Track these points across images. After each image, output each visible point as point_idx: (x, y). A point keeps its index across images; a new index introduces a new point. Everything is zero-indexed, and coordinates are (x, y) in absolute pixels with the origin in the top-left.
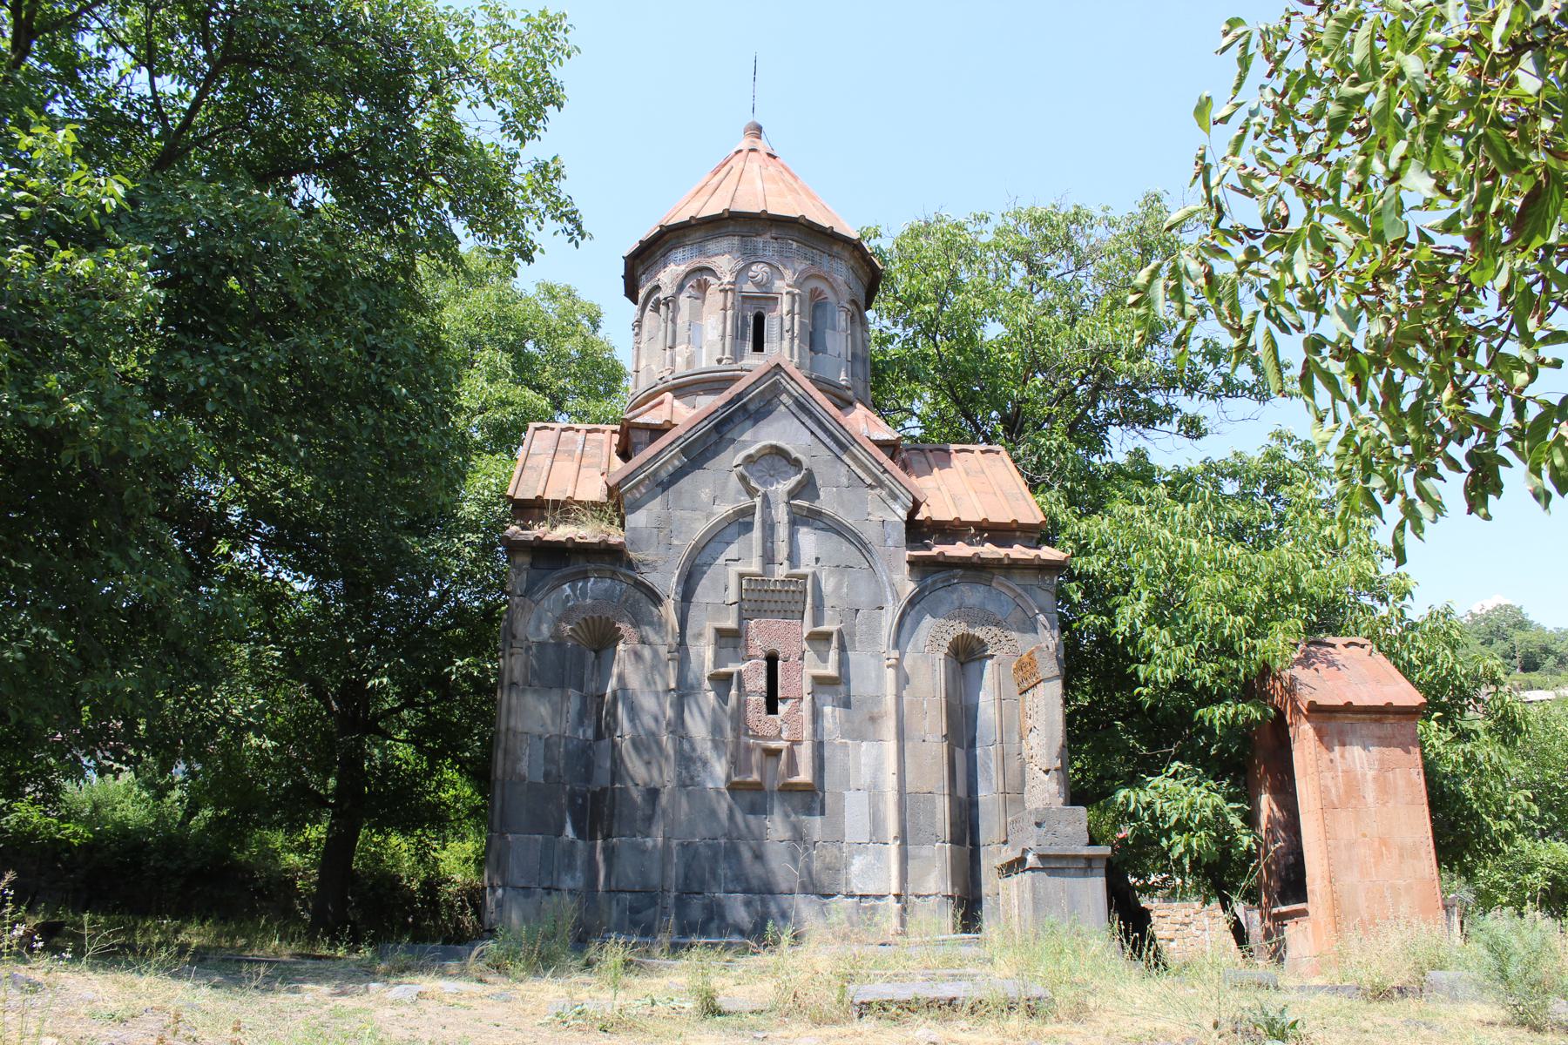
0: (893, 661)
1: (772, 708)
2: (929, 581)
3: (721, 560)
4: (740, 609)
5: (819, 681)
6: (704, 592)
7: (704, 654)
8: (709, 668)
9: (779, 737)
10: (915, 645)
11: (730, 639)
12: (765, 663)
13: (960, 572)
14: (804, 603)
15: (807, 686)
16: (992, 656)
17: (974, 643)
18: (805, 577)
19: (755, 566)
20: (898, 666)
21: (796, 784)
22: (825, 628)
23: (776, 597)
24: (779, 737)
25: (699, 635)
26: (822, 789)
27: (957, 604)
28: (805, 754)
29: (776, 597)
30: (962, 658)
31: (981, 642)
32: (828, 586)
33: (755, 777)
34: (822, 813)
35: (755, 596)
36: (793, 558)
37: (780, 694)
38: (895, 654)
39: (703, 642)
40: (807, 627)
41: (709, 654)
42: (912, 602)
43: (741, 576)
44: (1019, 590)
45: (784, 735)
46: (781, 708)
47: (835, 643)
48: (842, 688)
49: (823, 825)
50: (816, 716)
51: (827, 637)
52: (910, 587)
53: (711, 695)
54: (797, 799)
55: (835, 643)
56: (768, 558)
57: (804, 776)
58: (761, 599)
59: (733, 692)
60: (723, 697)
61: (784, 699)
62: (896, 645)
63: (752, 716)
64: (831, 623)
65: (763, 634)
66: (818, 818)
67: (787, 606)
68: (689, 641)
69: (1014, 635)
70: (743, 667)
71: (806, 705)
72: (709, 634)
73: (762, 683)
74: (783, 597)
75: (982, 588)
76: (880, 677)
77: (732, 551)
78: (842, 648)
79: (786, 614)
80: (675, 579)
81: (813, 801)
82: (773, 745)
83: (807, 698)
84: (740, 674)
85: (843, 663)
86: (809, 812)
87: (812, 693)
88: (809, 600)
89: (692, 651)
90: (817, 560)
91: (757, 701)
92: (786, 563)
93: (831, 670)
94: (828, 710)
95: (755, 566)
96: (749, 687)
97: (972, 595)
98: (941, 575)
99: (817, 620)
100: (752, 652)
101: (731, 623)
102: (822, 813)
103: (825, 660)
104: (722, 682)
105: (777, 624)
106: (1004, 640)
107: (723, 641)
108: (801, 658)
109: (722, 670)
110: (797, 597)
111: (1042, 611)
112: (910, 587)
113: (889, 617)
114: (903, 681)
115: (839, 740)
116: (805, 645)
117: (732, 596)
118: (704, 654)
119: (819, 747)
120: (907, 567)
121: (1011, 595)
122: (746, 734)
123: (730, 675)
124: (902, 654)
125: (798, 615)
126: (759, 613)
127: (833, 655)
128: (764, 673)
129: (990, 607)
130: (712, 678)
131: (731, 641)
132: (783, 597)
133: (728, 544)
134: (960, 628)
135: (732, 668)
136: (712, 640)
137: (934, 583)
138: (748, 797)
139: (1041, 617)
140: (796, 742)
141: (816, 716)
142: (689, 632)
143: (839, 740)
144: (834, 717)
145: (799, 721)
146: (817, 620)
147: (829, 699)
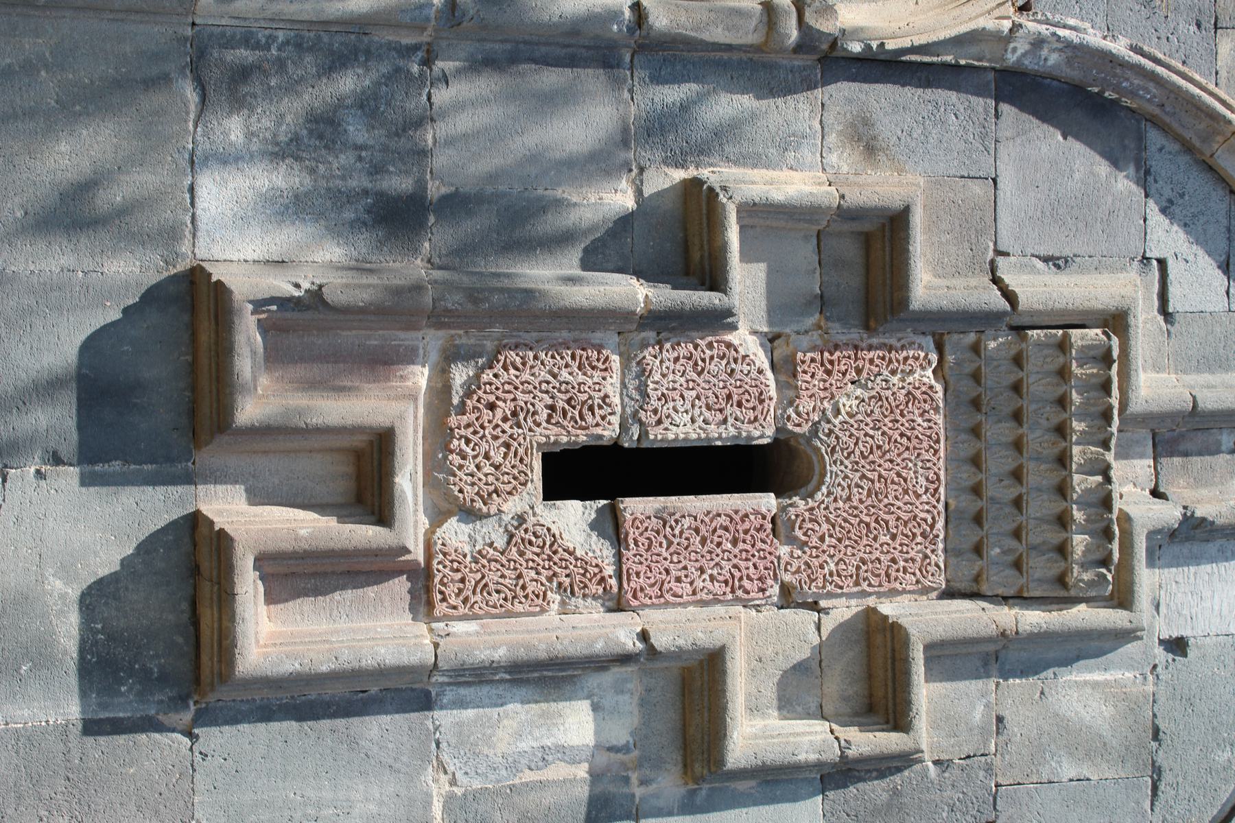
1: (569, 474)
3: (1167, 238)
4: (982, 320)
5: (693, 689)
6: (1045, 162)
7: (794, 160)
8: (744, 182)
9: (446, 506)
11: (858, 271)
12: (763, 434)
14: (1020, 599)
15: (677, 627)
18: (1123, 598)
19: (1155, 385)
21: (226, 597)
22: (925, 694)
23: (1038, 475)
24: (446, 506)
25: (866, 141)
26: (207, 717)
28: (373, 631)
29: (1038, 475)
32: (1084, 695)
33: (248, 411)
34: (92, 727)
35: (1038, 385)
36: (1193, 538)
37: (635, 507)
39: (842, 160)
40: (925, 617)
41: (795, 183)
43: (1116, 321)
45: (455, 533)
46: (573, 519)
47: (867, 741)
48: (669, 784)
49: (28, 739)
50: (546, 676)
51: (885, 703)
53: (620, 198)
54: (155, 609)
55: (867, 741)
56: (1179, 435)
57: (269, 635)
58: (1028, 403)
59: (635, 292)
60: (610, 248)
61: (611, 527)
63: (534, 375)
64: (946, 721)
65: (880, 414)
66: (74, 710)
67: (998, 525)
68: (842, 92)
70: (746, 339)
71: (591, 627)
72: (879, 187)
73: (682, 427)
74: (1040, 506)
77: (1199, 281)
78: (838, 774)
79: (970, 520)
80: (1094, 38)
81: (148, 682)
82: (408, 482)
83: (622, 632)
84: (720, 320)
85: (776, 780)
86: (101, 666)
87: (649, 652)
88: (1033, 619)
89: (797, 111)
90: (1177, 646)
91: (608, 400)
92: (1169, 513)
93: (756, 730)
94: (576, 724)
95: (1155, 385)
96: (665, 364)
99: (953, 657)
100: (810, 380)
101: (929, 284)
102: (92, 727)
103: (788, 704)
104: (683, 242)
105: (924, 479)
107: (850, 250)
108: (788, 598)
109: (733, 236)
110: (1041, 567)
115: (437, 789)
116: (842, 611)
117: (1037, 288)
118: (794, 160)
119: (405, 691)
122: (452, 356)
123: (715, 279)
125: (967, 569)
126: (968, 404)
127: (811, 738)
128: (720, 433)
130: (699, 203)
131: (851, 281)
132: (1040, 506)
133: (1225, 268)
135: (747, 283)
136: (858, 197)
138: (157, 370)
140: (423, 597)
141: (546, 676)
142: (881, 99)
143: (437, 789)
144: (544, 756)
145: (515, 598)
146: (953, 657)
147: (620, 734)
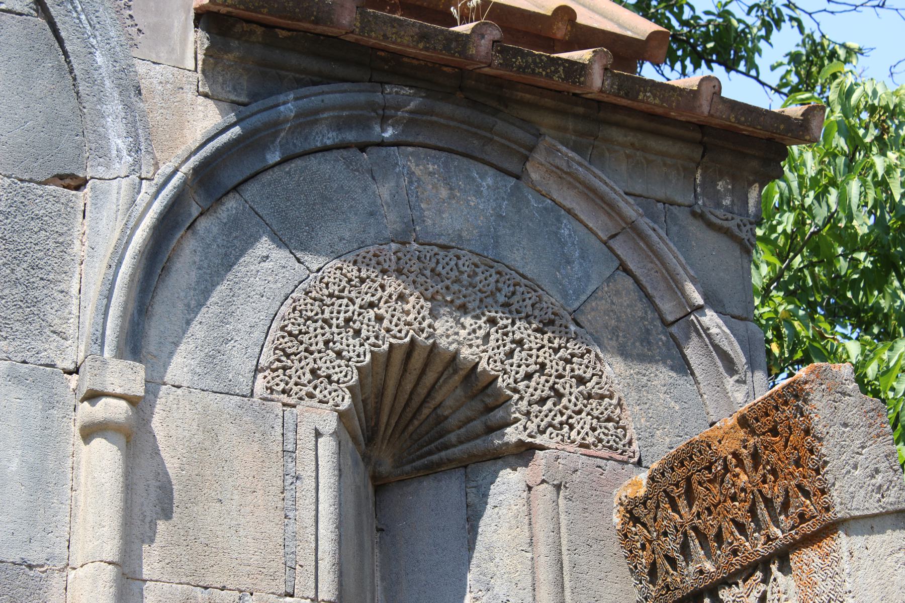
0: (113, 410)
2: (289, 106)
10: (213, 360)
13: (408, 98)
16: (524, 453)
17: (450, 395)
20: (133, 437)
27: (392, 221)
30: (386, 466)
31: (483, 395)
38: (126, 377)
42: (212, 178)
44: (630, 210)
52: (202, 122)
62: (133, 344)
69: (614, 370)
75: (489, 180)
76: (45, 481)
97: (457, 201)
98: (332, 97)
106: (571, 391)
111: (713, 301)
112: (202, 122)
113: (109, 225)
114: (148, 500)
120: (193, 43)
121: (599, 223)
124: (153, 385)
129: (522, 257)
134: (403, 315)
137: (307, 119)
139: (711, 319)
